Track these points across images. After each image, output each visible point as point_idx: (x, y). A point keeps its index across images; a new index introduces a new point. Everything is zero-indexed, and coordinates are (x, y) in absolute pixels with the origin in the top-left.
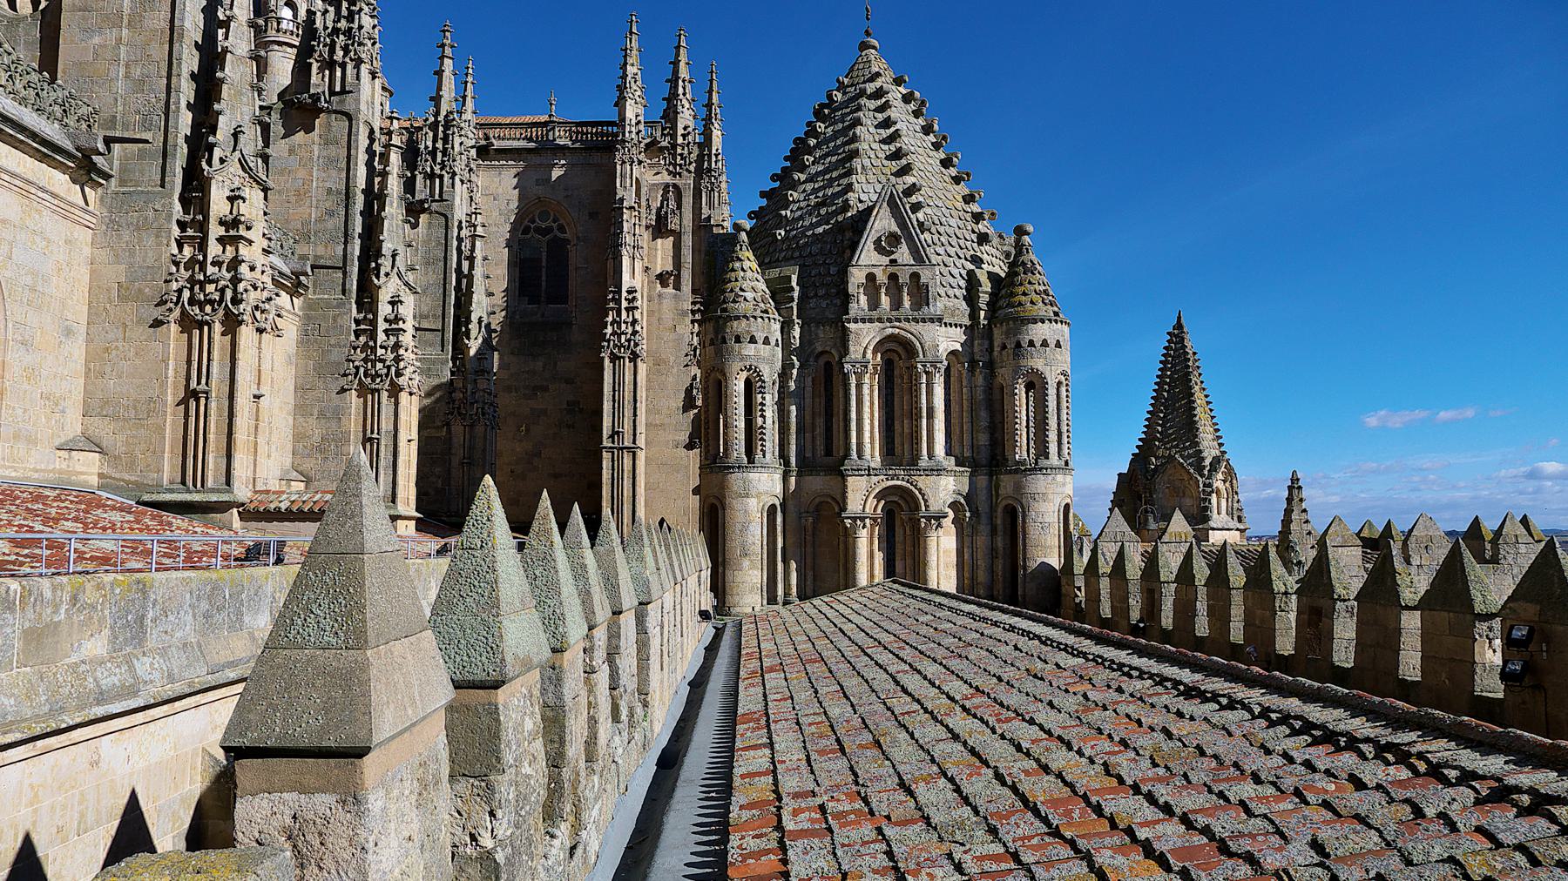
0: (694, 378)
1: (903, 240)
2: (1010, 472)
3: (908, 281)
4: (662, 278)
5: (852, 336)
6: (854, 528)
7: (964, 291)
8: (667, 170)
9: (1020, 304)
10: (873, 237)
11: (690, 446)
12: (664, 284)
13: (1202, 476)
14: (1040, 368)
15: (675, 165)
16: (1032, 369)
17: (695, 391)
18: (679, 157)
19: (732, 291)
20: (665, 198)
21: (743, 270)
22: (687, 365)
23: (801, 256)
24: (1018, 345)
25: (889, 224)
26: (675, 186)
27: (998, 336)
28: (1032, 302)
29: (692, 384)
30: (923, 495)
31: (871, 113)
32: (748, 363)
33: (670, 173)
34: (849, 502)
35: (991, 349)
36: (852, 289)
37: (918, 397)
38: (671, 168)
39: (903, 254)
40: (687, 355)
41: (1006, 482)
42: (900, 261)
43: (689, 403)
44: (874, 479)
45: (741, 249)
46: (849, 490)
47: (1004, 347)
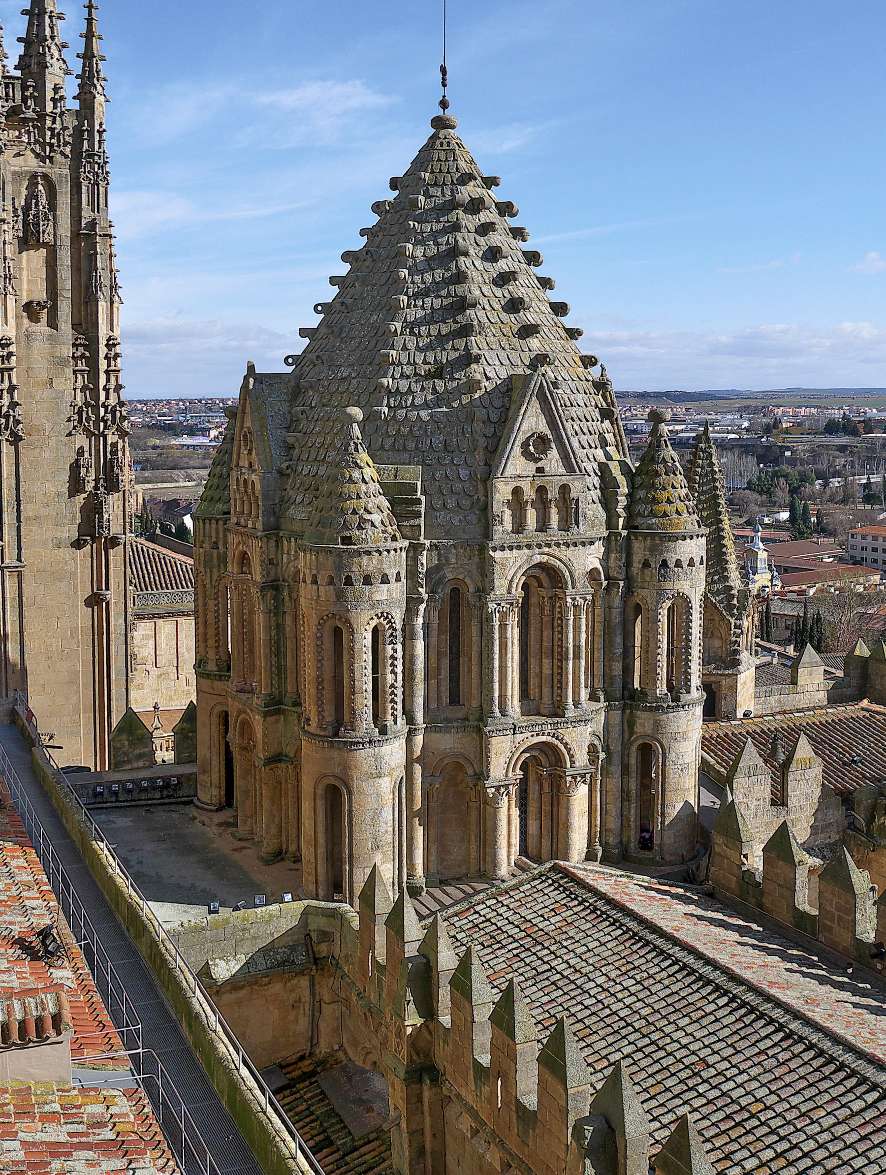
0: (80, 452)
1: (553, 445)
2: (645, 709)
3: (557, 496)
4: (31, 310)
5: (497, 568)
6: (496, 799)
7: (598, 490)
8: (33, 151)
9: (665, 515)
10: (521, 438)
11: (78, 544)
12: (34, 317)
13: (732, 615)
14: (686, 592)
15: (43, 145)
16: (678, 593)
17: (83, 471)
18: (48, 133)
19: (355, 512)
20: (32, 196)
21: (364, 480)
22: (70, 434)
23: (417, 448)
24: (664, 564)
25: (537, 423)
26: (45, 177)
27: (639, 551)
28: (678, 512)
29: (77, 461)
30: (569, 750)
31: (472, 236)
32: (380, 611)
33: (37, 156)
34: (492, 768)
35: (628, 564)
36: (497, 507)
37: (562, 632)
38: (38, 149)
39: (553, 461)
40: (69, 420)
41: (644, 722)
42: (547, 469)
43: (76, 485)
44: (519, 737)
45: (357, 450)
46: (492, 754)
47: (646, 564)
